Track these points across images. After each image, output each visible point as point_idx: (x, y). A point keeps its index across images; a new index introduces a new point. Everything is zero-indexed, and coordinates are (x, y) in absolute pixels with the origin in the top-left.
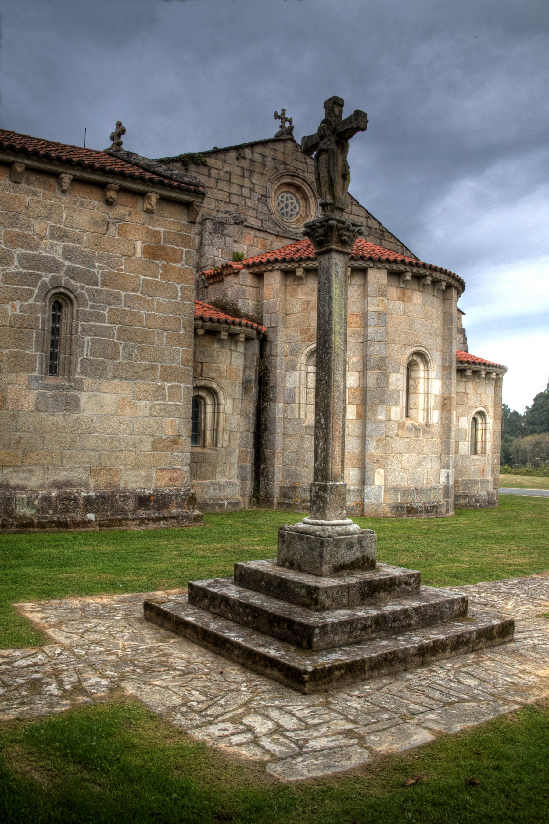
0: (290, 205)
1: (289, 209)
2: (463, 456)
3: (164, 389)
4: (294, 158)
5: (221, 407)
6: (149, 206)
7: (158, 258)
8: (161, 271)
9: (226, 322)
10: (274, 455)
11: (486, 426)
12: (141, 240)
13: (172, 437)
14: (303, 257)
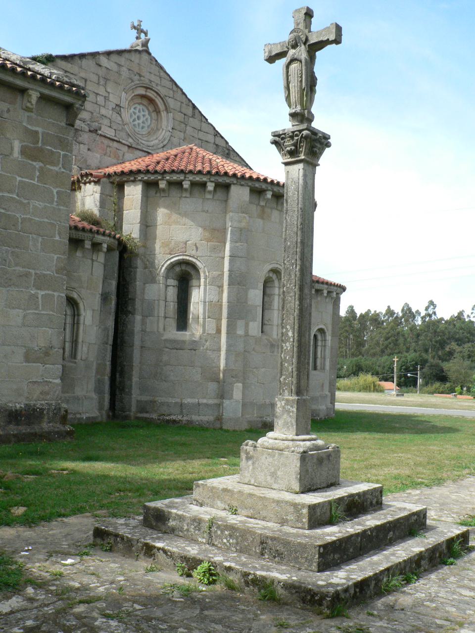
0: (142, 117)
1: (140, 121)
3: (38, 298)
5: (82, 318)
6: (29, 105)
7: (35, 158)
8: (38, 174)
9: (91, 231)
10: (132, 368)
11: (325, 343)
12: (19, 139)
13: (43, 349)
14: (167, 170)
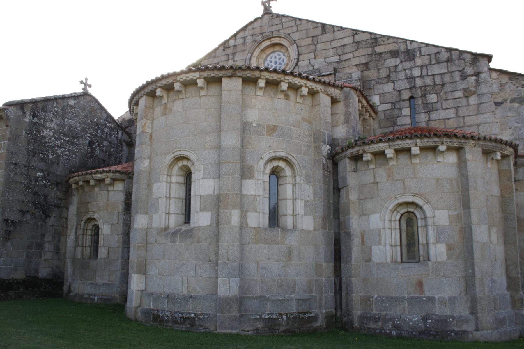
2: (378, 264)
4: (270, 25)
